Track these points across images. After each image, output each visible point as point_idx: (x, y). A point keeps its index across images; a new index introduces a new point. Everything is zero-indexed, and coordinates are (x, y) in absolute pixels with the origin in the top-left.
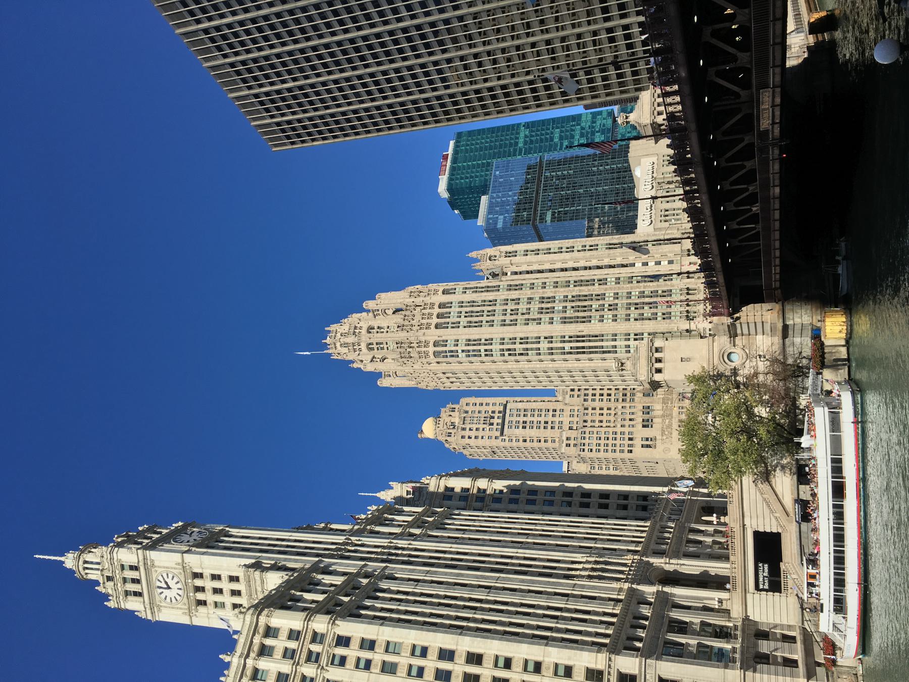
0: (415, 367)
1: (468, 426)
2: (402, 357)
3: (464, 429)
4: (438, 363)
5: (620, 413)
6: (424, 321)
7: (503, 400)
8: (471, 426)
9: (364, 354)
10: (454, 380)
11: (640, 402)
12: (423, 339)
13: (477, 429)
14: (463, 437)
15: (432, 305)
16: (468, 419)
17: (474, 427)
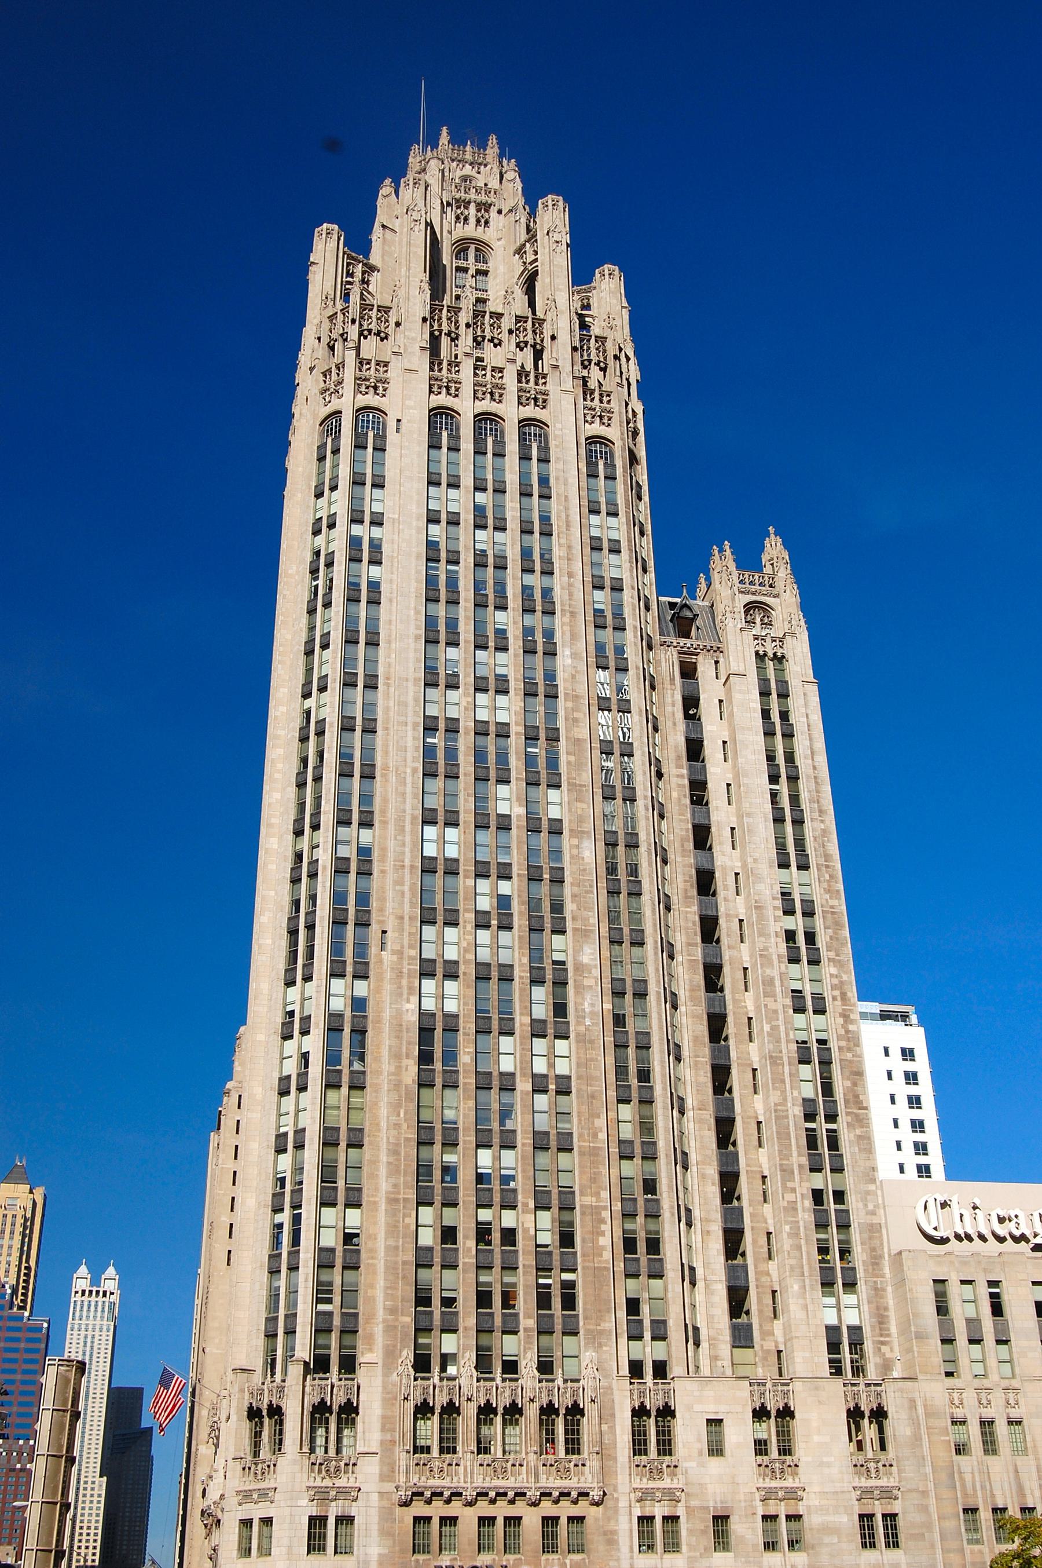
15: (541, 401)
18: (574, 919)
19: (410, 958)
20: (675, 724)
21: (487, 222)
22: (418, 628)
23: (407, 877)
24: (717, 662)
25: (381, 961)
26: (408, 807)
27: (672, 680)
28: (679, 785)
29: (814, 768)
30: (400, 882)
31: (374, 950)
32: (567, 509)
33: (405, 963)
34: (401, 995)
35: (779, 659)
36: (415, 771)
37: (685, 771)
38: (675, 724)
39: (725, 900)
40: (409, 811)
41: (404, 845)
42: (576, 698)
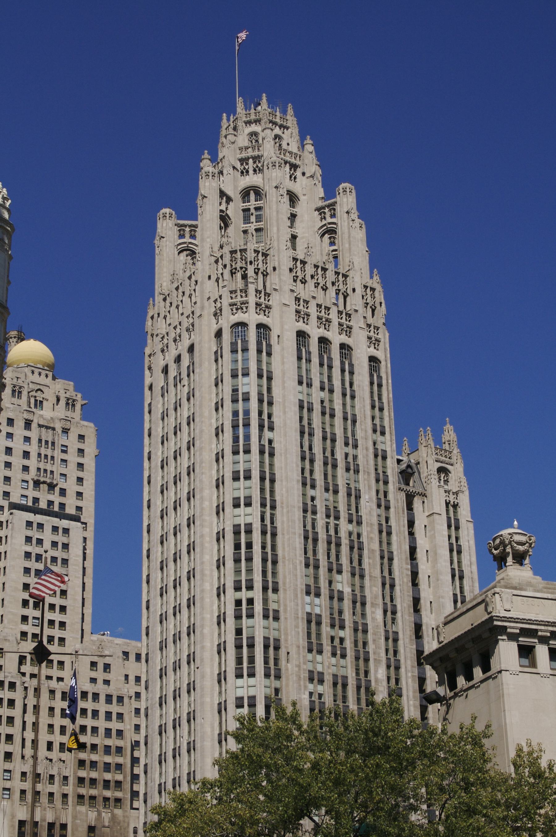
0: (210, 286)
1: (34, 434)
2: (233, 252)
3: (28, 424)
4: (219, 334)
5: (54, 772)
6: (312, 310)
7: (89, 516)
8: (35, 441)
9: (235, 180)
10: (173, 372)
11: (75, 817)
12: (274, 301)
13: (26, 455)
14: (10, 422)
16: (47, 435)
17: (33, 449)
18: (374, 653)
19: (304, 669)
20: (405, 538)
21: (295, 178)
22: (298, 476)
23: (300, 624)
24: (423, 502)
25: (287, 669)
26: (299, 583)
27: (403, 511)
28: (407, 575)
29: (471, 572)
30: (297, 626)
31: (283, 663)
32: (364, 406)
33: (302, 672)
34: (300, 689)
35: (455, 506)
36: (301, 562)
37: (409, 567)
38: (405, 538)
39: (428, 643)
40: (299, 586)
41: (297, 605)
42: (372, 525)
